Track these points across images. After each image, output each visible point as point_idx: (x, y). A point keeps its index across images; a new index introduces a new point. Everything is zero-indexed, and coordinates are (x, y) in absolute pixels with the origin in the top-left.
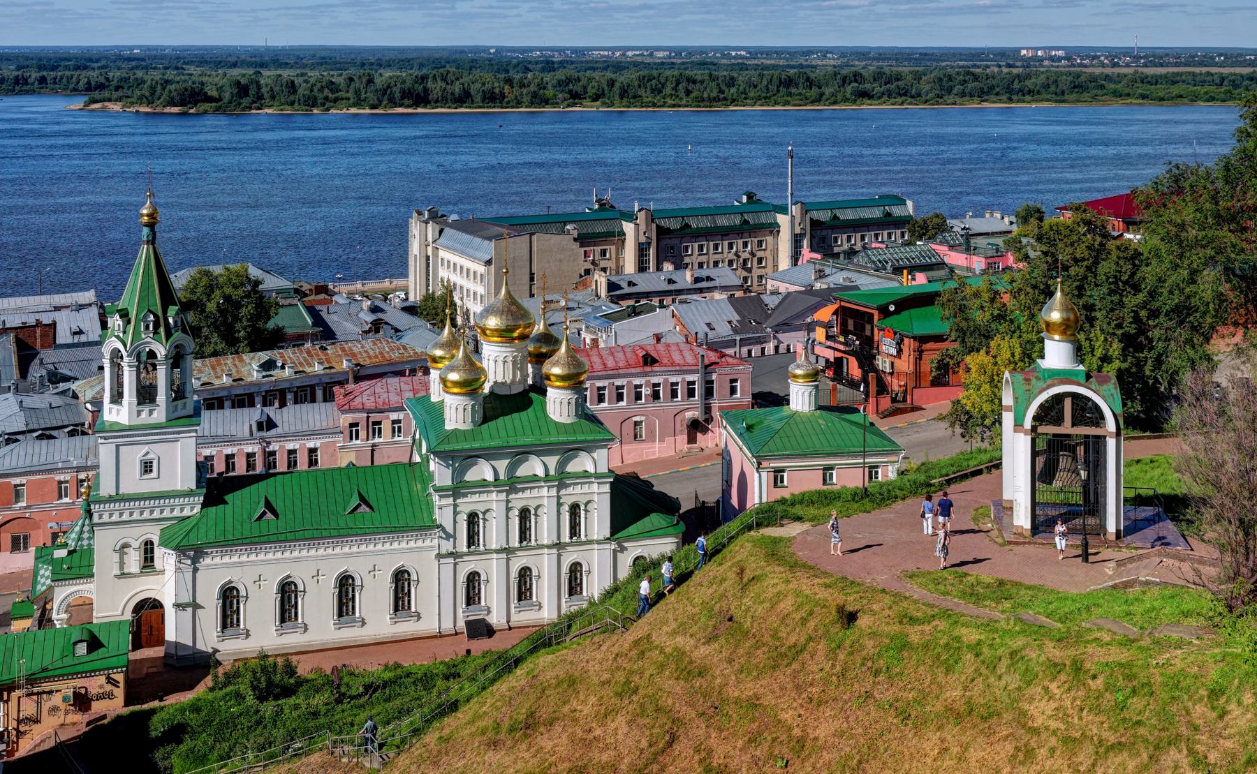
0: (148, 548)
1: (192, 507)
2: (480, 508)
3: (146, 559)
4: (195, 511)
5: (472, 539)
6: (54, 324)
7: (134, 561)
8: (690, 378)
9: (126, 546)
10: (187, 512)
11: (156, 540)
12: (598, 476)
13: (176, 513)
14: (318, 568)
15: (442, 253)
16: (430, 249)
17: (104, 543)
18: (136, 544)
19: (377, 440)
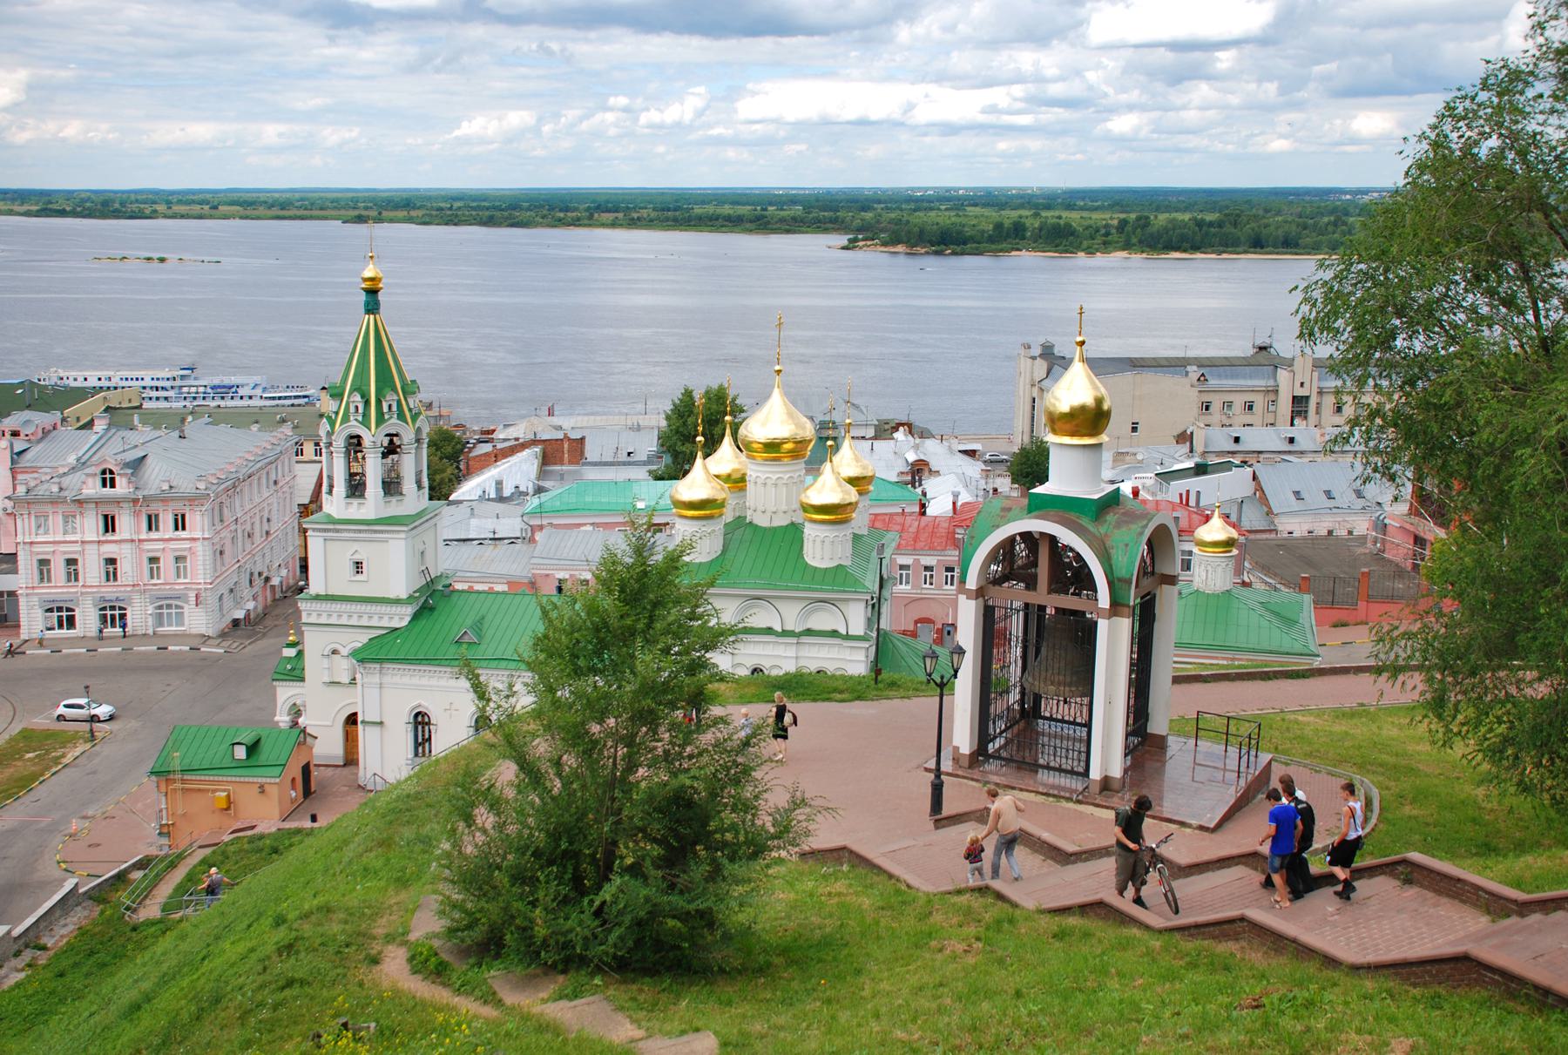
1: (400, 617)
4: (404, 623)
9: (334, 652)
10: (396, 624)
13: (385, 623)
17: (315, 644)
18: (345, 652)
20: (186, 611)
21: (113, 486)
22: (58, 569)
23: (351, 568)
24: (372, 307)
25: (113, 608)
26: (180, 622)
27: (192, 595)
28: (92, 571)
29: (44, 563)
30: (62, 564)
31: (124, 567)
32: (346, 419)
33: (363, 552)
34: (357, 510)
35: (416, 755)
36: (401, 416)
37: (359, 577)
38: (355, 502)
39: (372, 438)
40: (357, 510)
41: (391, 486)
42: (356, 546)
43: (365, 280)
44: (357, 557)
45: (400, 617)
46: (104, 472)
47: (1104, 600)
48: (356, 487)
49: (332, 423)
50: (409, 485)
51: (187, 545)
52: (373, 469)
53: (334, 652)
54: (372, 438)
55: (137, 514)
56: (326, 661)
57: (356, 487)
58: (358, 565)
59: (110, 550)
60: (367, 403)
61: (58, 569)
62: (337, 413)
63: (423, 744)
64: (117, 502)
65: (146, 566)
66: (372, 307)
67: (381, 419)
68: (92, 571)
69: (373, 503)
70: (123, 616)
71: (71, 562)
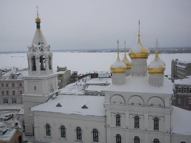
21: (14, 78)
22: (5, 93)
23: (33, 88)
24: (38, 27)
25: (14, 100)
28: (11, 93)
29: (3, 92)
30: (6, 92)
31: (16, 93)
37: (35, 91)
44: (35, 86)
46: (12, 76)
55: (18, 83)
59: (13, 89)
61: (5, 93)
63: (48, 132)
64: (14, 81)
65: (20, 92)
68: (11, 93)
70: (16, 101)
71: (7, 92)
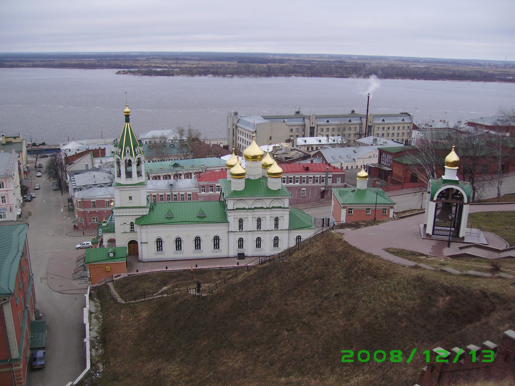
0: (132, 224)
2: (243, 217)
3: (131, 228)
5: (241, 226)
6: (105, 148)
7: (128, 228)
8: (322, 176)
9: (125, 223)
11: (134, 222)
12: (284, 208)
13: (141, 214)
14: (188, 233)
15: (238, 128)
16: (234, 127)
17: (118, 222)
19: (211, 192)
20: (6, 213)
26: (5, 217)
27: (8, 208)
32: (125, 155)
33: (132, 194)
34: (129, 181)
35: (157, 250)
36: (140, 153)
37: (131, 201)
38: (129, 179)
39: (134, 160)
40: (129, 181)
41: (139, 174)
42: (130, 192)
43: (125, 112)
45: (146, 212)
47: (466, 201)
48: (129, 175)
49: (120, 156)
50: (143, 174)
51: (5, 192)
52: (134, 169)
53: (125, 223)
54: (134, 160)
56: (122, 227)
57: (129, 175)
58: (130, 198)
60: (131, 150)
62: (121, 153)
66: (127, 120)
67: (136, 155)
69: (135, 179)
